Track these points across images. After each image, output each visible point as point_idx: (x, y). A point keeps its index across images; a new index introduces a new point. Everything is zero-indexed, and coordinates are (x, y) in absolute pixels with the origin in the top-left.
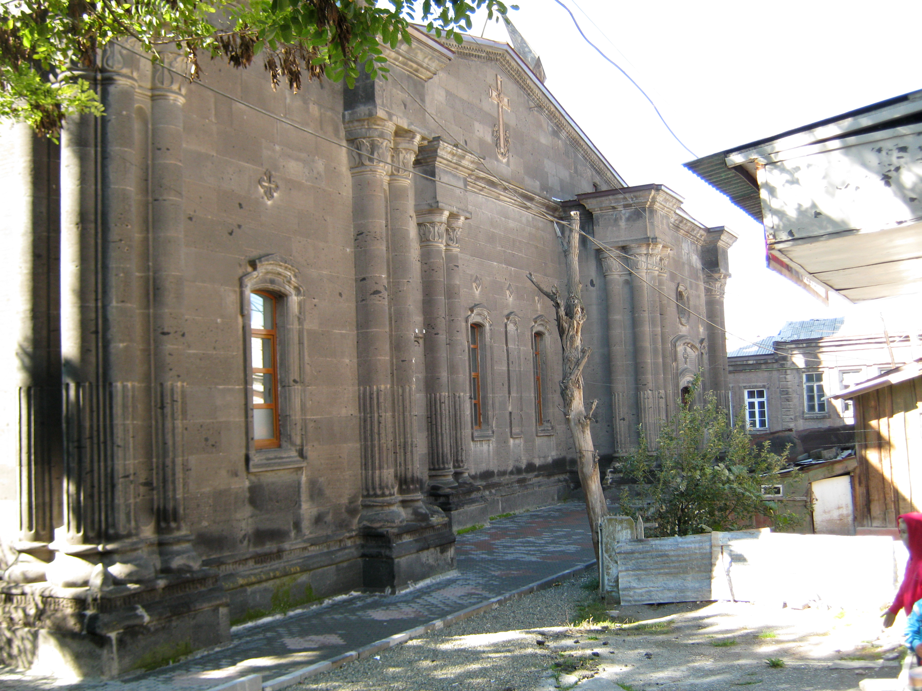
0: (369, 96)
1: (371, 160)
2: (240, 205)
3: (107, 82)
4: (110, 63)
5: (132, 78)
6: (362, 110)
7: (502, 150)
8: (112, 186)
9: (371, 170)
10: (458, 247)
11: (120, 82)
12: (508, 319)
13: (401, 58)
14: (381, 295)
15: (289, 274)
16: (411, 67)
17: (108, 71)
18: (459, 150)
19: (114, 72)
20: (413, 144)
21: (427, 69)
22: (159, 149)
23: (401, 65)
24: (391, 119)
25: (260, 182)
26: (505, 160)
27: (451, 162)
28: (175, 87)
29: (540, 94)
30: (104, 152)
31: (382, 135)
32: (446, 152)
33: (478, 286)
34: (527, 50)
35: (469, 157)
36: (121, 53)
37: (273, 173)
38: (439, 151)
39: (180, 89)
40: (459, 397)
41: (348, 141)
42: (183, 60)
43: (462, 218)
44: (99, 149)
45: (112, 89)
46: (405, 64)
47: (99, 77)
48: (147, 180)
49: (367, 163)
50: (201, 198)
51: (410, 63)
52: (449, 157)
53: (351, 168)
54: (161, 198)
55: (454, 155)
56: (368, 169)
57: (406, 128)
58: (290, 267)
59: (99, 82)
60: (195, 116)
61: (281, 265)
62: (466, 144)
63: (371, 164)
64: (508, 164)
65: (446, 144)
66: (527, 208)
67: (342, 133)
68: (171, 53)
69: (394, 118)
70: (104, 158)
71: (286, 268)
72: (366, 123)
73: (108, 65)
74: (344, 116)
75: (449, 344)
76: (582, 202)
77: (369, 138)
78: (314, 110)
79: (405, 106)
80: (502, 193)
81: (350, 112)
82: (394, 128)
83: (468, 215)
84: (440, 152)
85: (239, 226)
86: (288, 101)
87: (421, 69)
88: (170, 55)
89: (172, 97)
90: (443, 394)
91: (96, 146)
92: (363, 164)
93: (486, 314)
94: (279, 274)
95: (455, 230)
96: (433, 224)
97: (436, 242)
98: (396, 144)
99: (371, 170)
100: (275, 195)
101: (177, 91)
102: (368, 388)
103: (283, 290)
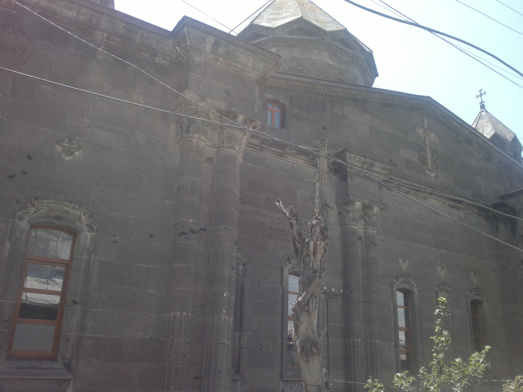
1: (188, 132)
2: (29, 157)
7: (430, 168)
10: (374, 230)
12: (439, 288)
14: (186, 236)
15: (79, 213)
26: (433, 175)
33: (405, 261)
35: (377, 164)
40: (375, 344)
43: (376, 209)
58: (77, 207)
61: (66, 205)
64: (436, 177)
65: (353, 155)
66: (458, 209)
71: (74, 208)
75: (367, 302)
76: (505, 202)
80: (429, 196)
83: (382, 207)
85: (24, 173)
90: (356, 340)
93: (413, 282)
94: (67, 212)
95: (369, 217)
96: (347, 212)
97: (351, 225)
100: (77, 153)
102: (168, 315)
103: (73, 226)
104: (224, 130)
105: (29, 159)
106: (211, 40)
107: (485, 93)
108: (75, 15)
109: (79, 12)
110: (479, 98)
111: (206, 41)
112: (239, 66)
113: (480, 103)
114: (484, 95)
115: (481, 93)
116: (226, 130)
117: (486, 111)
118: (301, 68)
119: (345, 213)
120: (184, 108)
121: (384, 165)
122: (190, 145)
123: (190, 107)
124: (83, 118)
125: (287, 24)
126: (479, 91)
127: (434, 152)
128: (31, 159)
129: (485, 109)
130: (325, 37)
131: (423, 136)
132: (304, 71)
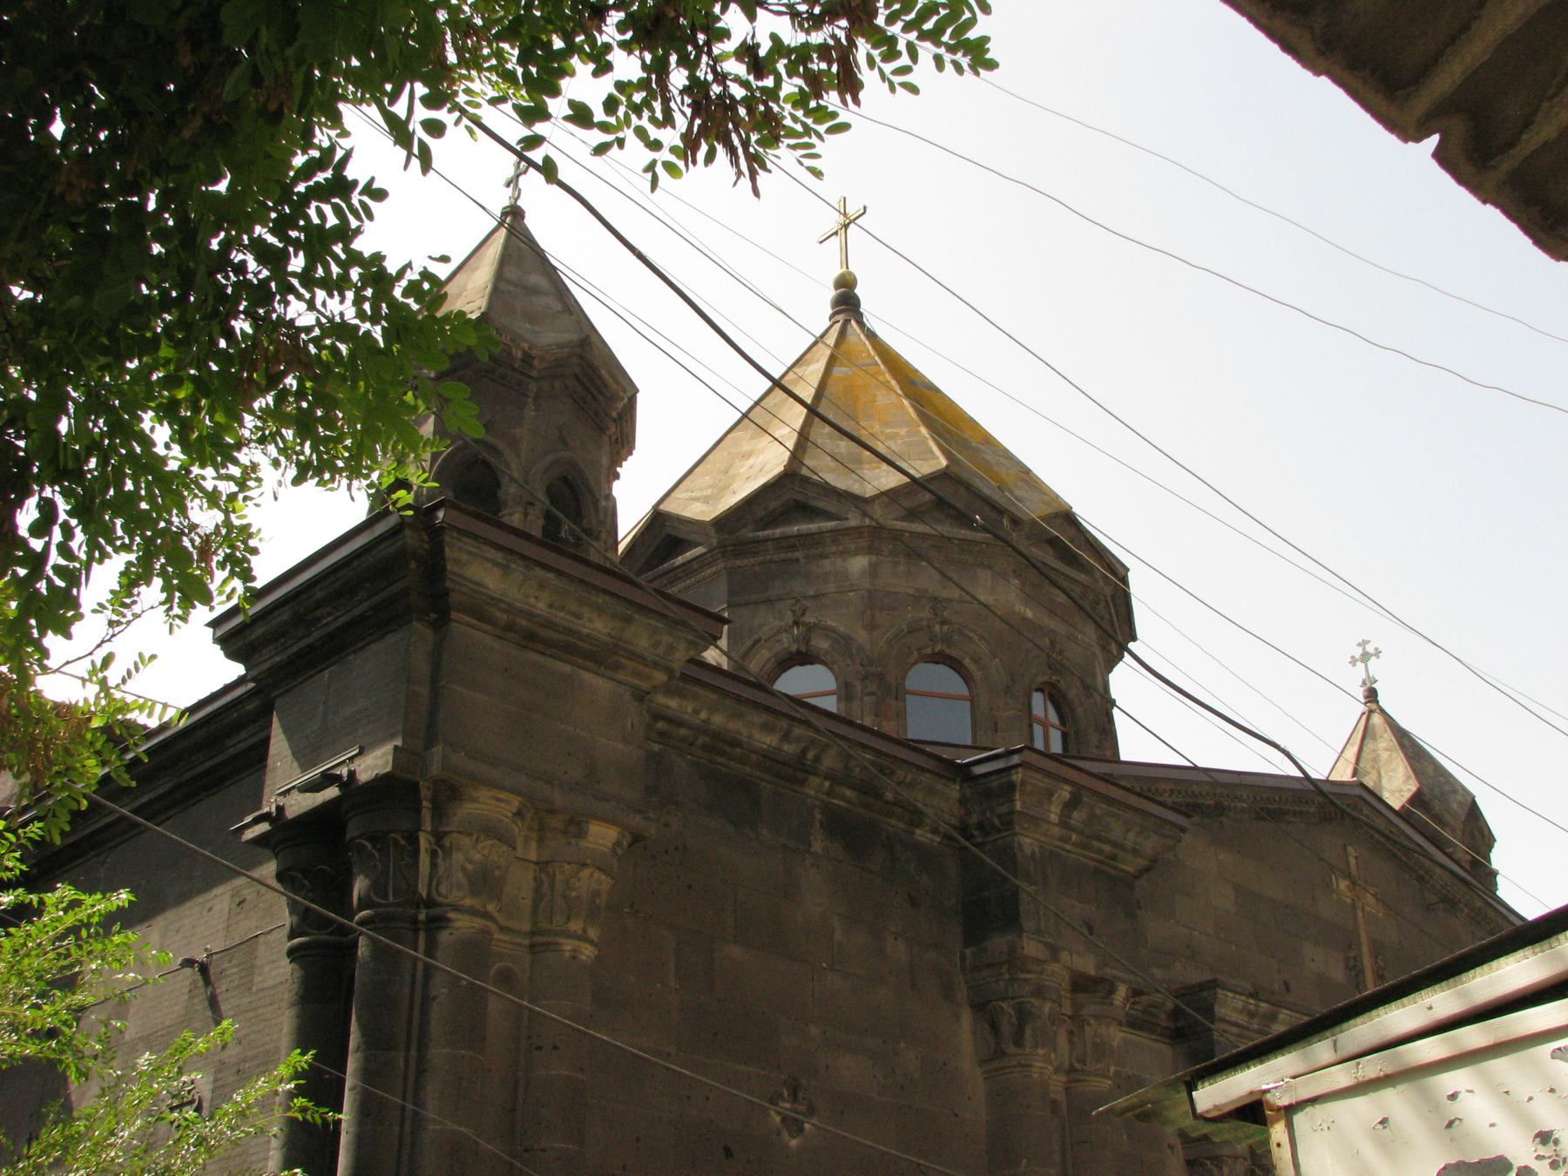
0: (1010, 918)
1: (1018, 1041)
2: (728, 1152)
3: (437, 925)
4: (443, 889)
5: (486, 915)
6: (998, 944)
8: (430, 1127)
9: (1020, 1065)
11: (458, 924)
13: (1074, 837)
16: (1101, 851)
17: (441, 905)
18: (1262, 1004)
19: (448, 905)
20: (1111, 1004)
21: (1136, 852)
22: (539, 1048)
23: (1078, 850)
24: (1055, 958)
25: (773, 1101)
27: (1248, 1029)
28: (575, 926)
29: (1447, 876)
30: (421, 1059)
31: (1039, 992)
32: (1235, 1009)
34: (1447, 788)
36: (464, 869)
37: (804, 1081)
38: (1217, 1008)
39: (584, 930)
41: (972, 1007)
42: (592, 875)
44: (413, 1053)
45: (444, 937)
46: (1084, 846)
47: (422, 916)
48: (513, 1110)
49: (1011, 1049)
50: (638, 1140)
51: (1096, 844)
52: (1242, 1019)
53: (982, 1062)
54: (536, 1146)
55: (1251, 1015)
56: (1015, 1063)
57: (1092, 972)
59: (420, 926)
60: (632, 978)
62: (1288, 990)
63: (1020, 1051)
67: (962, 993)
68: (569, 863)
69: (1064, 956)
70: (421, 1071)
72: (1004, 969)
73: (439, 894)
74: (963, 958)
77: (1013, 998)
78: (898, 951)
79: (1090, 929)
81: (973, 949)
82: (1066, 975)
84: (1220, 1011)
86: (838, 936)
87: (1121, 854)
88: (567, 867)
89: (568, 945)
91: (408, 1049)
92: (1004, 1054)
98: (1076, 1006)
99: (1020, 1065)
101: (580, 932)
104: (1083, 1026)
105: (727, 1158)
106: (1064, 793)
107: (1378, 653)
108: (774, 744)
109: (786, 737)
110: (1360, 665)
111: (1054, 798)
112: (1107, 848)
113: (1364, 683)
114: (1373, 658)
115: (1364, 649)
116: (1089, 1024)
117: (1383, 712)
118: (945, 628)
119: (1208, 1163)
120: (1007, 976)
121: (1298, 1016)
122: (1026, 1076)
123: (1023, 976)
124: (807, 1025)
125: (904, 488)
126: (1359, 645)
127: (1377, 948)
128: (731, 1155)
129: (1377, 702)
130: (1014, 535)
131: (1349, 900)
132: (955, 637)
